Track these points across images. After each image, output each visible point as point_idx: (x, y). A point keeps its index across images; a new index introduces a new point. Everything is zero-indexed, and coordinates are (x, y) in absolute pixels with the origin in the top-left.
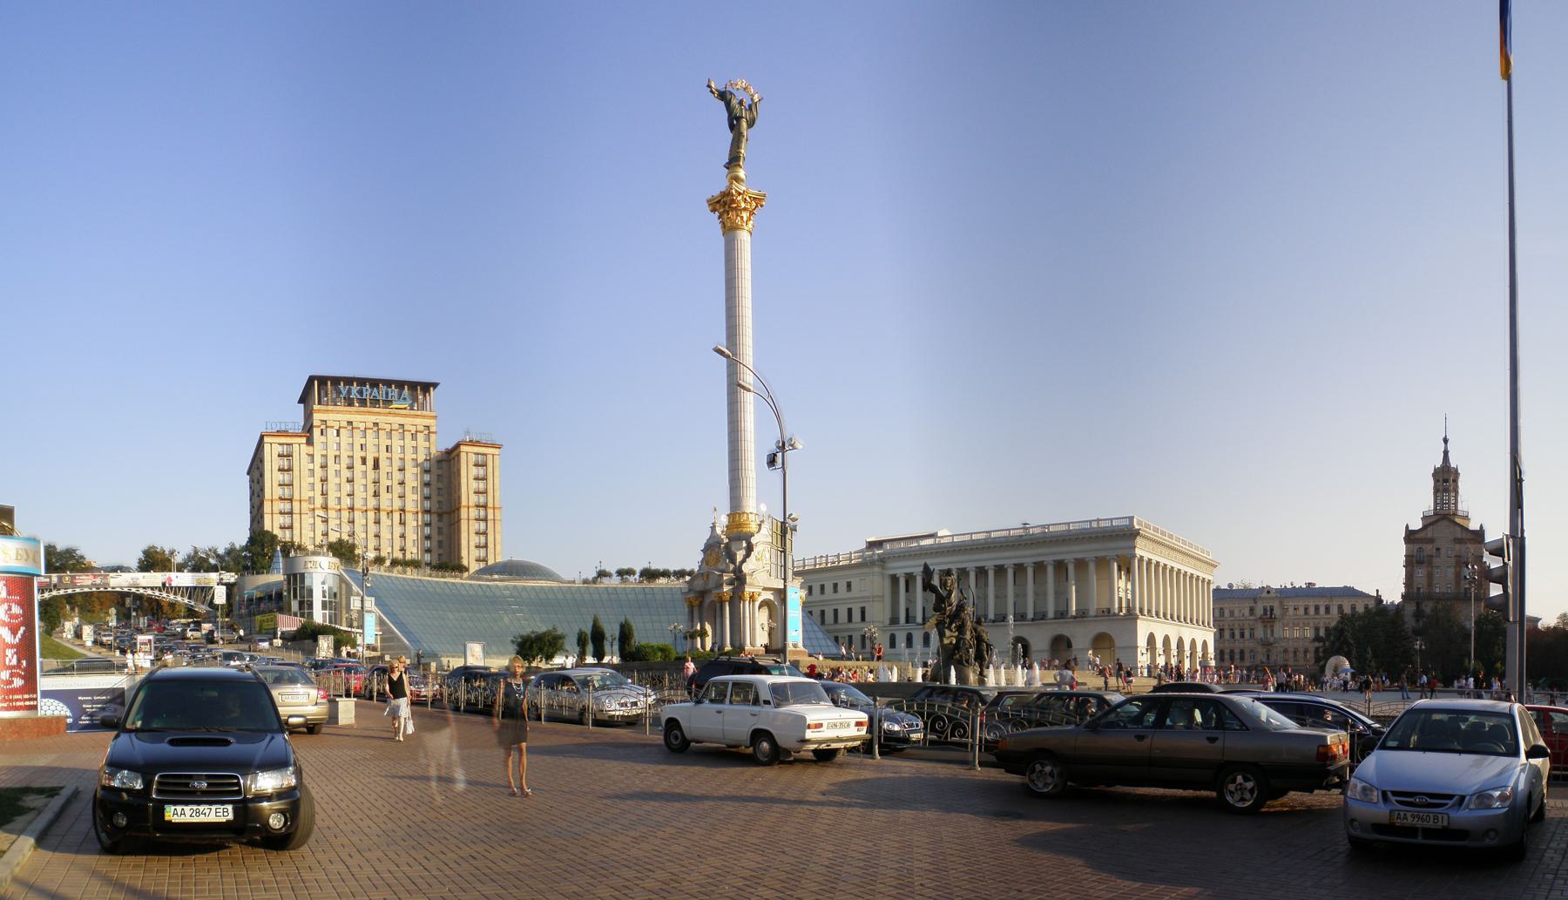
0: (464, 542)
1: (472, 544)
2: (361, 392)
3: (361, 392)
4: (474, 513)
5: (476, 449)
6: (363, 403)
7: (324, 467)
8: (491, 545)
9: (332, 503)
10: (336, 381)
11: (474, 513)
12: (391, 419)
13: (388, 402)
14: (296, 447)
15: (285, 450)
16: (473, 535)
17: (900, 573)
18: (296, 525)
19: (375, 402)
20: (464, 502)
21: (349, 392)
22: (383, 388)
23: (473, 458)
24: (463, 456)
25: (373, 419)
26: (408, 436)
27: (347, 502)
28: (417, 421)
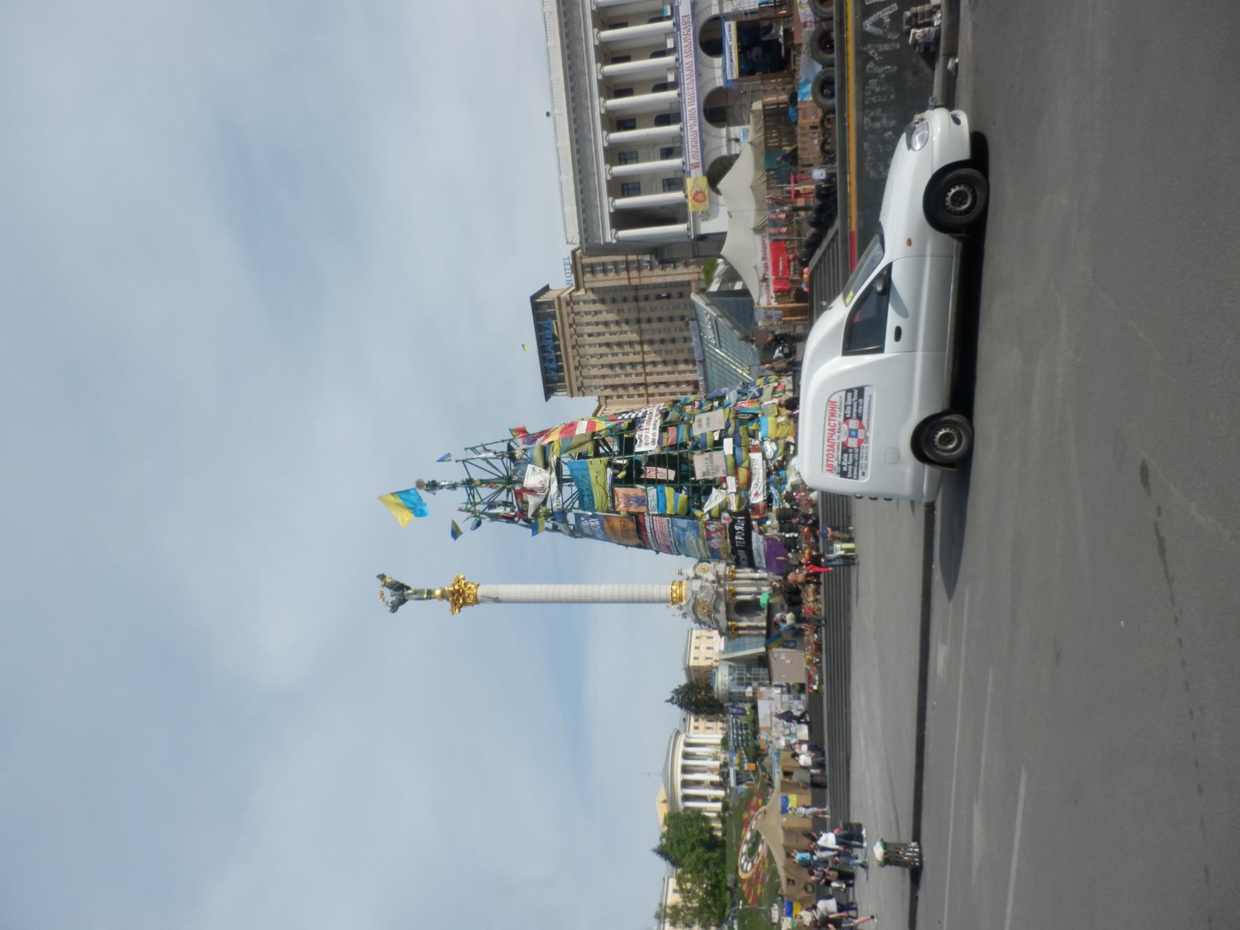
0: (660, 280)
2: (551, 361)
3: (551, 361)
4: (634, 274)
5: (580, 274)
6: (558, 358)
9: (640, 380)
11: (634, 274)
12: (568, 335)
13: (555, 338)
19: (557, 348)
20: (626, 282)
21: (552, 369)
23: (588, 276)
24: (587, 285)
25: (569, 349)
26: (578, 318)
28: (564, 312)
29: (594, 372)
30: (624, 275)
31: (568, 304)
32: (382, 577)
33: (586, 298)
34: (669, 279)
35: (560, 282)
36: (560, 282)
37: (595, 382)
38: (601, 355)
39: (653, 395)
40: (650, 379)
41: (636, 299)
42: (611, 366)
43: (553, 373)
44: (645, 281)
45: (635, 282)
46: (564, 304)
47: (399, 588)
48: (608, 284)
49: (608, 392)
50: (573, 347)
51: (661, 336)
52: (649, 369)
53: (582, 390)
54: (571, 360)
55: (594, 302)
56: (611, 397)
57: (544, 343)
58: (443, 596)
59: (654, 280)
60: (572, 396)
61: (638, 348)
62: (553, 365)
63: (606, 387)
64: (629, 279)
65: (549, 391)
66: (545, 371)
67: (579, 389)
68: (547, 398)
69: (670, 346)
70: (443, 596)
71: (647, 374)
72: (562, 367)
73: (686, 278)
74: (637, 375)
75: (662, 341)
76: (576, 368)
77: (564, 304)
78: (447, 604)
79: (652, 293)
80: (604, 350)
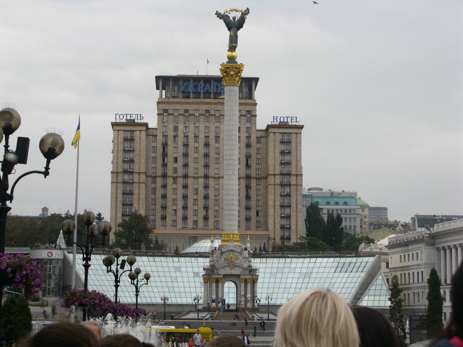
0: (271, 203)
1: (278, 203)
2: (195, 87)
4: (278, 180)
5: (282, 130)
6: (197, 95)
7: (165, 145)
8: (293, 205)
9: (170, 172)
10: (177, 80)
11: (278, 180)
14: (137, 134)
15: (128, 135)
16: (278, 198)
17: (441, 246)
18: (136, 191)
19: (207, 95)
21: (187, 86)
22: (213, 84)
23: (279, 137)
24: (271, 135)
25: (206, 107)
27: (181, 172)
29: (181, 127)
30: (277, 172)
31: (249, 112)
32: (247, 12)
33: (253, 131)
34: (271, 211)
35: (269, 108)
36: (269, 108)
37: (171, 127)
38: (196, 137)
39: (154, 182)
40: (170, 181)
41: (248, 177)
42: (186, 145)
43: (182, 88)
44: (271, 189)
45: (271, 180)
46: (249, 108)
47: (240, 24)
48: (271, 155)
49: (160, 139)
50: (207, 111)
51: (211, 196)
52: (180, 181)
53: (163, 113)
54: (194, 107)
55: (249, 137)
56: (155, 141)
57: (213, 84)
58: (232, 59)
59: (271, 197)
60: (158, 103)
61: (201, 173)
62: (191, 88)
63: (165, 136)
64: (275, 175)
65: (163, 82)
66: (186, 79)
67: (166, 111)
68: (158, 78)
69: (201, 204)
70: (232, 59)
71: (175, 179)
72: (188, 97)
73: (271, 227)
74: (175, 170)
75: (206, 197)
76: (186, 111)
77: (249, 108)
78: (226, 60)
79: (253, 193)
80: (202, 141)
